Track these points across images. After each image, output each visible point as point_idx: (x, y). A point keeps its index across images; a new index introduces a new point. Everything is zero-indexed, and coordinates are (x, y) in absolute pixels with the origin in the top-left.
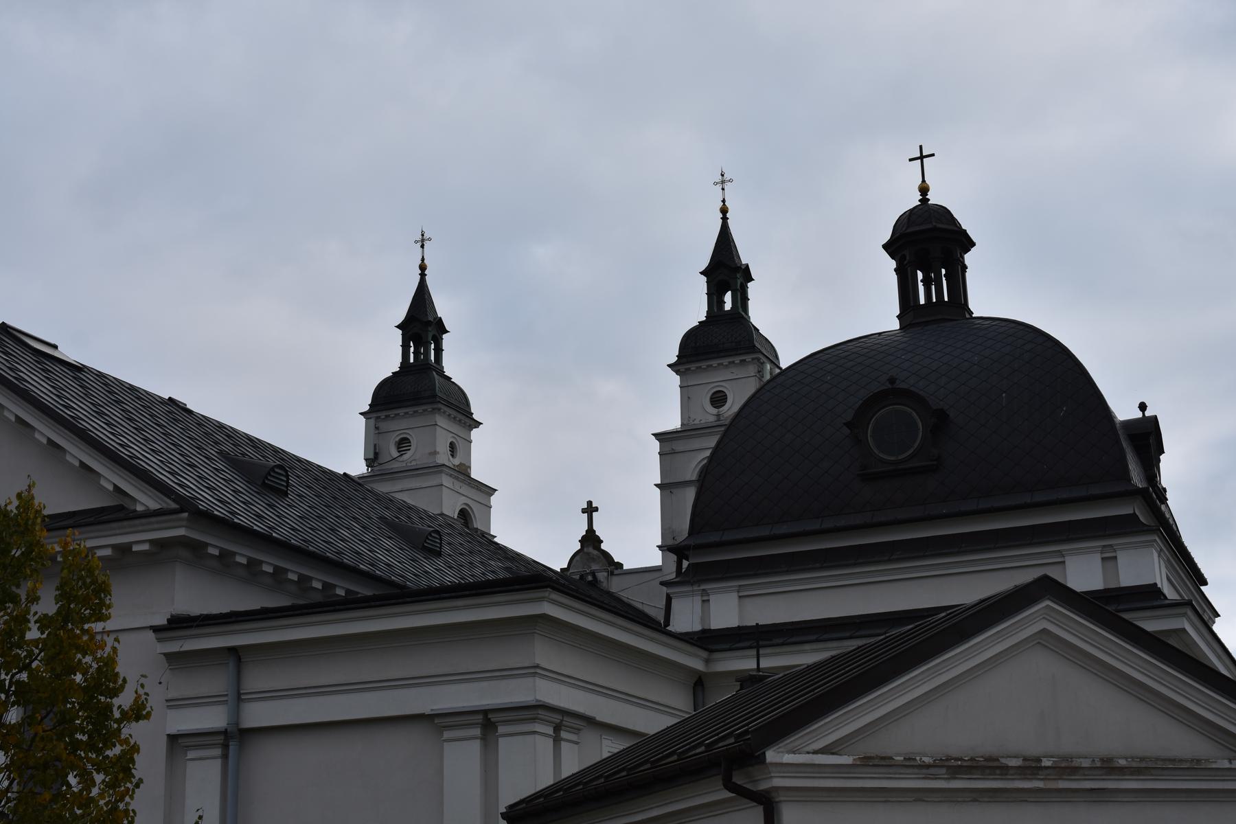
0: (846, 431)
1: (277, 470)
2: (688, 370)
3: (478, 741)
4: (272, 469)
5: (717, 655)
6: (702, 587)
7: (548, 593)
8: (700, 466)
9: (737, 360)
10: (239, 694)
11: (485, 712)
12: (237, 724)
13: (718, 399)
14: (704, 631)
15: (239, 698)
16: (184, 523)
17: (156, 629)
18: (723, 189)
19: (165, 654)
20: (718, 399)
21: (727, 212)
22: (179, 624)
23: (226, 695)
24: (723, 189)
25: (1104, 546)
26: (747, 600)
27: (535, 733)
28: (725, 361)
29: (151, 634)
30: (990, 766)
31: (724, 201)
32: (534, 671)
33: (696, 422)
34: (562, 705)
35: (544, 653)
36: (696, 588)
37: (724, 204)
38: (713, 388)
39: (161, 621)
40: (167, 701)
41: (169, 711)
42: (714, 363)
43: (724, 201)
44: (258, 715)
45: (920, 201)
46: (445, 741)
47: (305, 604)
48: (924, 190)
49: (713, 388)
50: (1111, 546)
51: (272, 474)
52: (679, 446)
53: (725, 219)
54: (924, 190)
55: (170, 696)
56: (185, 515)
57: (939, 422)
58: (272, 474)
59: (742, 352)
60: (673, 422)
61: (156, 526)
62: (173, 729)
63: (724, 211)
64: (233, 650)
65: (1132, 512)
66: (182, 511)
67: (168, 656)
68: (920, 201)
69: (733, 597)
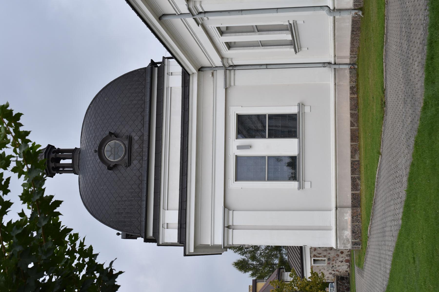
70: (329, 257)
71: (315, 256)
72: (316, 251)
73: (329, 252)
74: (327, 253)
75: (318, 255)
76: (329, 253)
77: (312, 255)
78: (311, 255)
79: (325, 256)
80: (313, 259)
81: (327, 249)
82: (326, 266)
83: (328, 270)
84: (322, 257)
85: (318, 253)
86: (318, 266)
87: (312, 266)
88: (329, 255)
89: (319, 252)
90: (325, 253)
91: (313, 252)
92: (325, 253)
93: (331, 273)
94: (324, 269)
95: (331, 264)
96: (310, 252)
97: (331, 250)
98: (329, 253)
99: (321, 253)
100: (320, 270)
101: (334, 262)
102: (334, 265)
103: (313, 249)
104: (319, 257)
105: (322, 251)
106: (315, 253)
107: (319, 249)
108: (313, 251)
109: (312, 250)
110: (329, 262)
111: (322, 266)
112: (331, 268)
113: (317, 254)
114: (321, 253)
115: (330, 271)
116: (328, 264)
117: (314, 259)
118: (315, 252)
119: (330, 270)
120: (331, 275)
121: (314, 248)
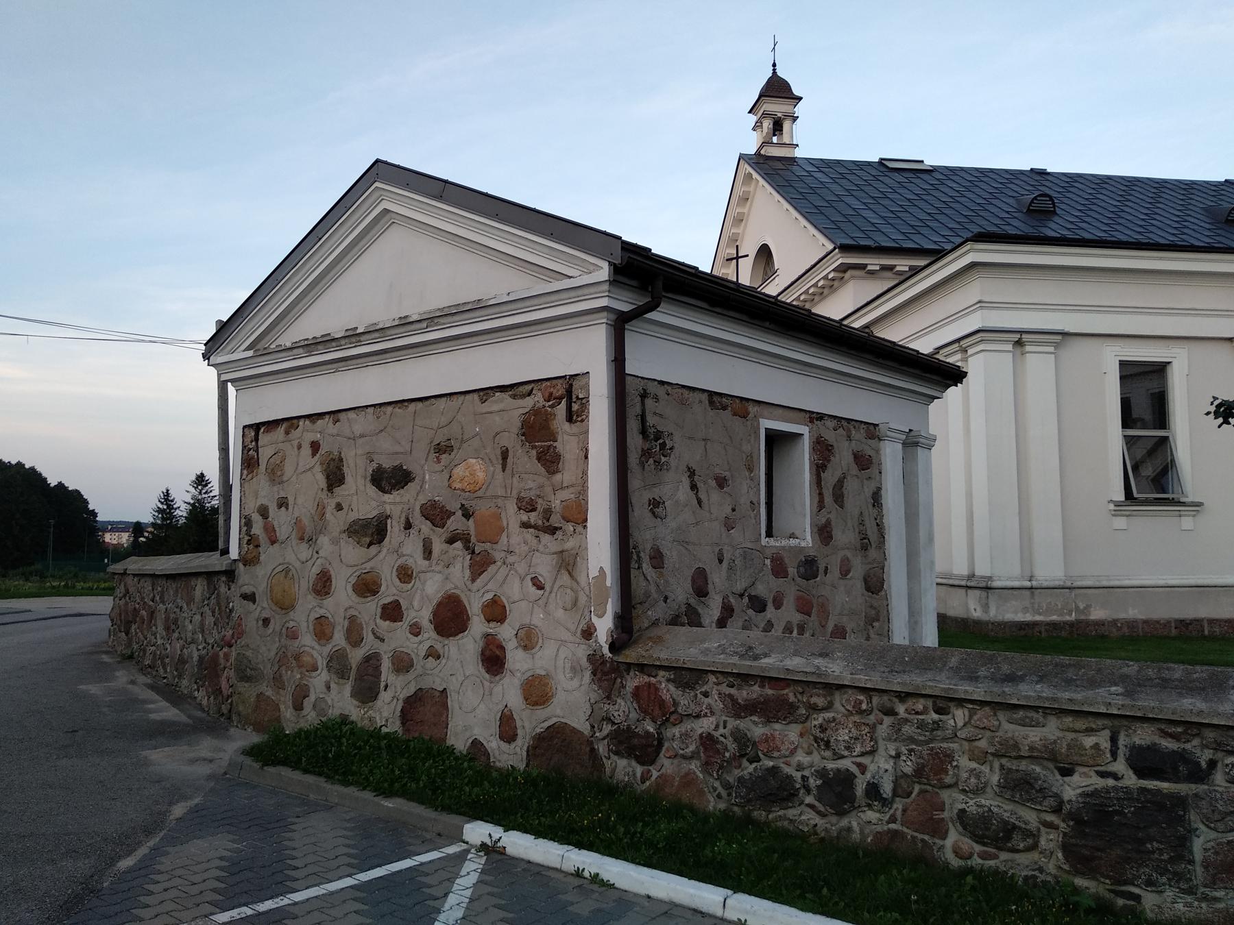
1: (1039, 198)
30: (326, 342)
51: (1035, 201)
56: (837, 250)
58: (1035, 201)
66: (835, 249)
70: (821, 570)
71: (823, 450)
72: (854, 470)
73: (858, 570)
74: (849, 555)
75: (830, 477)
76: (845, 573)
77: (830, 436)
79: (824, 533)
81: (873, 553)
82: (759, 539)
83: (727, 556)
84: (821, 505)
85: (840, 484)
87: (753, 409)
88: (835, 572)
89: (851, 486)
90: (844, 536)
91: (847, 443)
92: (844, 536)
93: (701, 587)
94: (729, 525)
95: (776, 584)
96: (849, 420)
97: (866, 580)
98: (845, 573)
99: (842, 507)
100: (721, 482)
101: (797, 618)
102: (770, 612)
103: (867, 448)
104: (818, 481)
105: (856, 512)
106: (843, 459)
107: (868, 490)
109: (859, 440)
110: (792, 571)
111: (754, 505)
112: (739, 587)
113: (838, 474)
114: (842, 507)
115: (717, 579)
117: (799, 436)
118: (851, 459)
119: (729, 578)
120: (688, 585)
121: (871, 453)
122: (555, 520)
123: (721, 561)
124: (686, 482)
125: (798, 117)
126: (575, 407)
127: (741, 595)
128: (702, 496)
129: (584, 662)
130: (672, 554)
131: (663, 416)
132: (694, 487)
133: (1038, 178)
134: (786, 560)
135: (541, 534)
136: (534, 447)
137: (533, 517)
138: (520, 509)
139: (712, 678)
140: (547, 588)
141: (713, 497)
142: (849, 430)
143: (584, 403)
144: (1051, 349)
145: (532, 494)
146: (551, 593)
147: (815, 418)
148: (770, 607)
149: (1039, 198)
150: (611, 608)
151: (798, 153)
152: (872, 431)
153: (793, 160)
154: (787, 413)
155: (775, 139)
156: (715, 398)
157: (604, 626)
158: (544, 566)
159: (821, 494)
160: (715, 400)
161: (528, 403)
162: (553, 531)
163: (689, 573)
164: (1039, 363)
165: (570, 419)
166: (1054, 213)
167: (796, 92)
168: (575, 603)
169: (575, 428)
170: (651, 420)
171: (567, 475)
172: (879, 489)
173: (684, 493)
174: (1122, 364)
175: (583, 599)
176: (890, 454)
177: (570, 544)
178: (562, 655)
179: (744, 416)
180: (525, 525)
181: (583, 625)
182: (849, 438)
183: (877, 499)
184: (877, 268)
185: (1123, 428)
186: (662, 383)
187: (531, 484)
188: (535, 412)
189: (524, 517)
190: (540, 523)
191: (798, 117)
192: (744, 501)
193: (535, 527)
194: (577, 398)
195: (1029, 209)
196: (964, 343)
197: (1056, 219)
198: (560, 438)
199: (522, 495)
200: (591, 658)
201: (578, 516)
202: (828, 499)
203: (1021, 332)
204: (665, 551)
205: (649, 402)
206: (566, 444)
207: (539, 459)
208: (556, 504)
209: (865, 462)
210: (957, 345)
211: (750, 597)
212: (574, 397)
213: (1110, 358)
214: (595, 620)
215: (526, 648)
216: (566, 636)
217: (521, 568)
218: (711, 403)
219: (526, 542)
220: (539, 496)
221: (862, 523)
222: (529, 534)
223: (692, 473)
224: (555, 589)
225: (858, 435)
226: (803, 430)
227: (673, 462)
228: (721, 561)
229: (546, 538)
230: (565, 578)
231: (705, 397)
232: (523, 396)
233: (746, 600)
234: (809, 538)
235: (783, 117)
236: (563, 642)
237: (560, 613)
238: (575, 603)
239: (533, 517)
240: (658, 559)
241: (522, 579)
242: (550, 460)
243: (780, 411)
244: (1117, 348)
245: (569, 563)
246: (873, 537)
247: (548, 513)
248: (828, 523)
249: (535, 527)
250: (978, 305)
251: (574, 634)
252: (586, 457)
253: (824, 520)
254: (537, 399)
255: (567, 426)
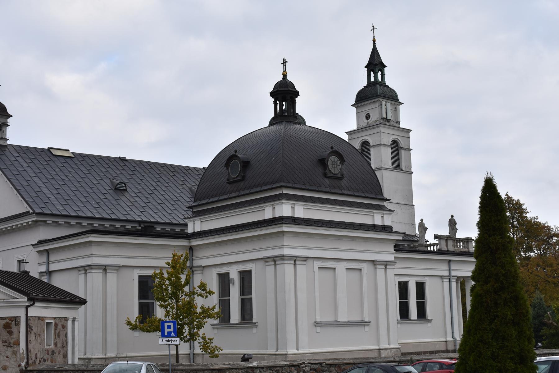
0: (225, 168)
1: (119, 184)
2: (358, 106)
3: (102, 273)
4: (118, 184)
5: (191, 241)
6: (193, 219)
7: (89, 235)
8: (361, 142)
9: (372, 101)
10: (48, 262)
11: (84, 267)
12: (48, 269)
13: (368, 117)
14: (194, 232)
15: (48, 264)
16: (35, 216)
17: (33, 245)
18: (374, 32)
19: (37, 251)
20: (368, 117)
21: (375, 41)
22: (41, 242)
23: (45, 262)
24: (374, 32)
25: (272, 204)
26: (202, 223)
27: (92, 272)
28: (369, 102)
29: (31, 246)
31: (374, 37)
32: (92, 255)
33: (361, 126)
34: (112, 263)
35: (95, 250)
36: (191, 219)
37: (374, 38)
38: (365, 113)
39: (35, 242)
40: (38, 264)
41: (39, 267)
42: (365, 103)
43: (374, 37)
44: (53, 267)
45: (282, 78)
46: (79, 274)
47: (90, 230)
48: (285, 76)
49: (365, 113)
50: (263, 206)
51: (118, 185)
52: (354, 136)
53: (374, 44)
54: (285, 76)
55: (39, 262)
56: (34, 214)
57: (246, 164)
58: (118, 185)
59: (374, 98)
60: (354, 127)
61: (31, 217)
62: (39, 272)
63: (374, 41)
64: (46, 250)
65: (282, 192)
66: (33, 213)
67: (38, 252)
68: (282, 78)
69: (199, 221)
71: (56, 325)
72: (62, 329)
73: (62, 353)
75: (57, 331)
76: (59, 353)
77: (57, 322)
78: (57, 319)
79: (56, 344)
80: (52, 321)
81: (65, 349)
84: (55, 338)
85: (59, 332)
86: (44, 332)
88: (57, 354)
89: (61, 333)
90: (60, 345)
91: (60, 323)
92: (60, 345)
96: (61, 317)
98: (59, 353)
105: (62, 339)
106: (60, 327)
108: (62, 323)
109: (63, 322)
110: (50, 353)
111: (44, 339)
112: (42, 356)
113: (59, 330)
114: (59, 338)
116: (47, 351)
117: (52, 323)
118: (61, 326)
122: (11, 345)
123: (39, 351)
124: (34, 335)
125: (9, 125)
126: (17, 323)
127: (42, 359)
128: (37, 338)
129: (19, 371)
130: (32, 350)
131: (32, 323)
132: (35, 337)
133: (121, 163)
134: (49, 351)
135: (8, 347)
136: (6, 330)
137: (6, 344)
138: (3, 342)
139: (45, 371)
140: (10, 358)
141: (38, 339)
142: (61, 320)
143: (19, 322)
144: (116, 271)
145: (6, 339)
146: (11, 359)
147: (55, 318)
148: (46, 361)
149: (119, 184)
150: (25, 361)
151: (9, 142)
152: (66, 319)
153: (6, 146)
154: (50, 318)
155: (31, 211)
156: (39, 318)
157: (23, 364)
158: (9, 354)
159: (55, 336)
160: (39, 318)
161: (5, 321)
162: (11, 347)
163: (35, 354)
164: (112, 277)
165: (16, 325)
166: (126, 190)
167: (9, 112)
168: (17, 360)
169: (17, 327)
170: (30, 324)
171: (15, 336)
172: (66, 333)
173: (34, 338)
174: (140, 276)
175: (18, 359)
176: (70, 323)
177: (15, 349)
178: (13, 370)
179: (43, 320)
180: (4, 346)
181: (18, 364)
182: (61, 322)
183: (66, 336)
184: (51, 222)
185: (139, 299)
186: (32, 317)
187: (5, 337)
188: (7, 323)
189: (4, 344)
190: (8, 345)
191: (9, 125)
192: (42, 339)
193: (7, 346)
194: (17, 321)
195: (115, 189)
196: (86, 268)
197: (126, 194)
198: (13, 328)
199: (3, 339)
200: (20, 370)
201: (17, 343)
202: (57, 336)
203: (106, 266)
204: (31, 350)
205: (30, 321)
206: (14, 329)
207: (7, 332)
208: (12, 341)
209: (64, 327)
210: (83, 268)
211: (43, 359)
212: (17, 321)
213: (136, 275)
214: (21, 363)
215: (4, 370)
216: (14, 367)
217: (3, 354)
218: (38, 319)
219: (4, 349)
220: (8, 340)
221: (63, 342)
222: (5, 347)
223: (35, 334)
224: (12, 358)
225: (63, 321)
226: (52, 321)
227: (33, 332)
228: (39, 351)
229: (9, 348)
230: (14, 356)
231: (37, 318)
232: (4, 320)
233: (42, 360)
234: (53, 346)
235: (2, 124)
236: (14, 368)
237: (13, 362)
238: (17, 360)
239: (6, 344)
240: (30, 351)
241: (3, 356)
242: (10, 333)
243: (49, 318)
244: (138, 271)
245: (15, 353)
246: (65, 345)
247: (10, 343)
248: (57, 342)
249: (7, 346)
250: (91, 256)
251: (16, 366)
252: (19, 332)
253: (56, 341)
254: (7, 320)
255: (15, 326)
